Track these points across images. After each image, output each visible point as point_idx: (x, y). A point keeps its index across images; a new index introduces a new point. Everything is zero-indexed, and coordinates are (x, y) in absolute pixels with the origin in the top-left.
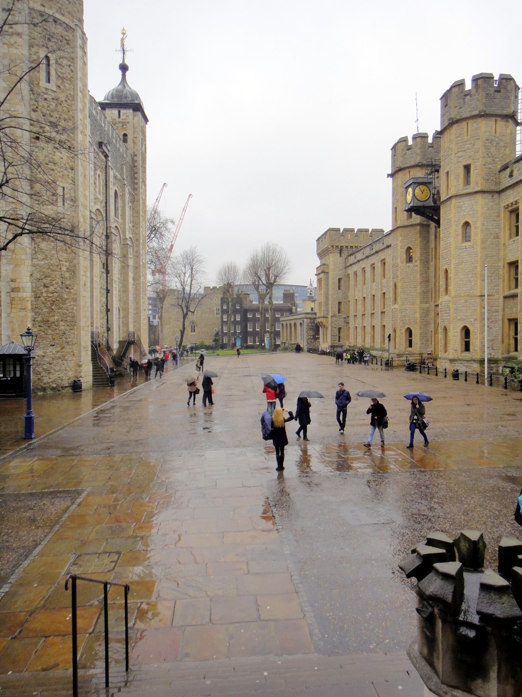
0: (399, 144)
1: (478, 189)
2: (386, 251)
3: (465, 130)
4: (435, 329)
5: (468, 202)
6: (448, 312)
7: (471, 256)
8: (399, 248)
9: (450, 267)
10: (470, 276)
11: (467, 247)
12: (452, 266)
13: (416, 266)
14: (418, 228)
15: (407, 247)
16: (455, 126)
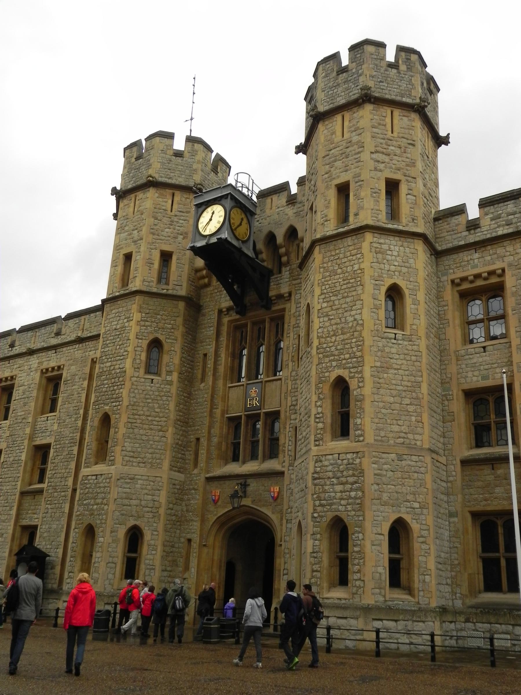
0: (158, 139)
1: (419, 230)
2: (20, 361)
3: (388, 120)
4: (201, 536)
5: (397, 248)
6: (351, 479)
7: (408, 358)
8: (132, 336)
9: (361, 372)
10: (407, 401)
11: (399, 336)
12: (367, 372)
13: (170, 383)
14: (181, 305)
15: (151, 337)
16: (369, 107)
